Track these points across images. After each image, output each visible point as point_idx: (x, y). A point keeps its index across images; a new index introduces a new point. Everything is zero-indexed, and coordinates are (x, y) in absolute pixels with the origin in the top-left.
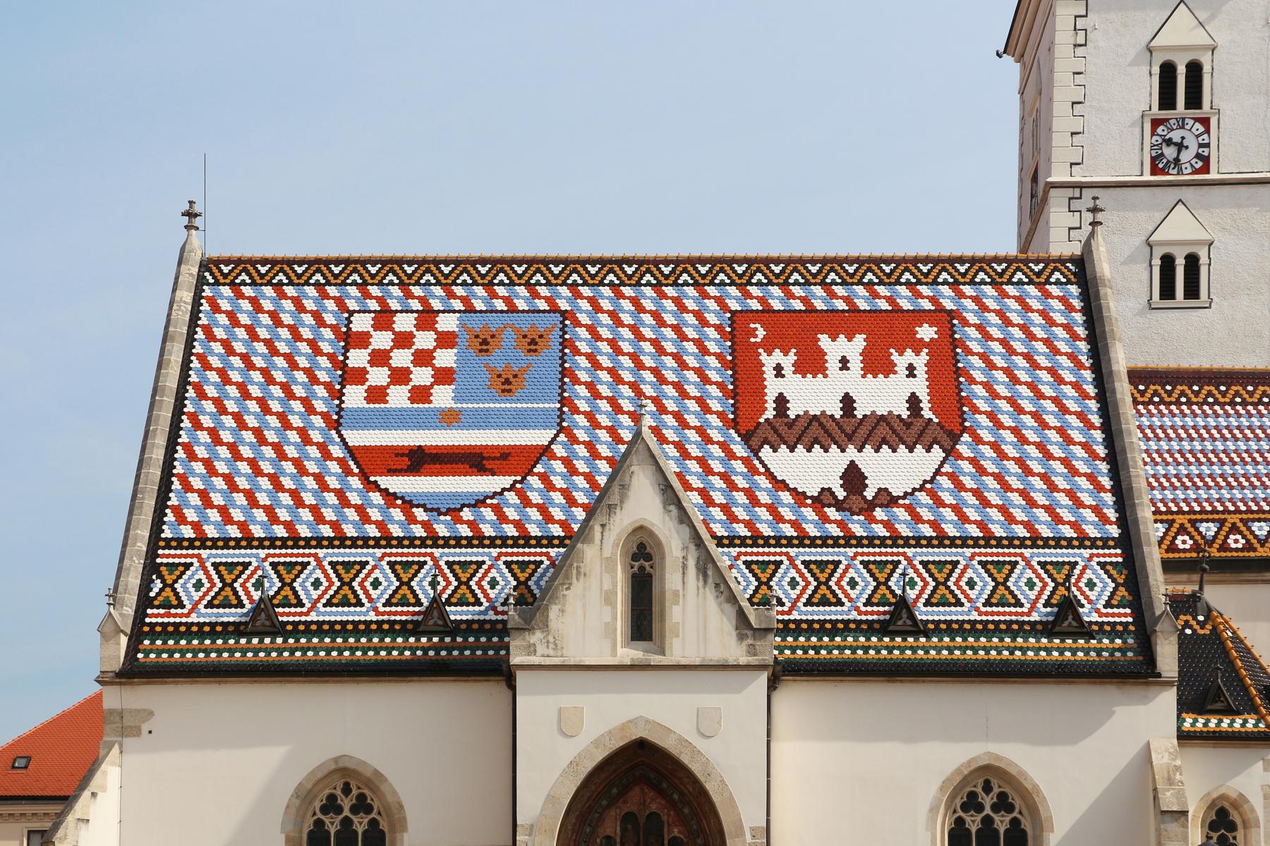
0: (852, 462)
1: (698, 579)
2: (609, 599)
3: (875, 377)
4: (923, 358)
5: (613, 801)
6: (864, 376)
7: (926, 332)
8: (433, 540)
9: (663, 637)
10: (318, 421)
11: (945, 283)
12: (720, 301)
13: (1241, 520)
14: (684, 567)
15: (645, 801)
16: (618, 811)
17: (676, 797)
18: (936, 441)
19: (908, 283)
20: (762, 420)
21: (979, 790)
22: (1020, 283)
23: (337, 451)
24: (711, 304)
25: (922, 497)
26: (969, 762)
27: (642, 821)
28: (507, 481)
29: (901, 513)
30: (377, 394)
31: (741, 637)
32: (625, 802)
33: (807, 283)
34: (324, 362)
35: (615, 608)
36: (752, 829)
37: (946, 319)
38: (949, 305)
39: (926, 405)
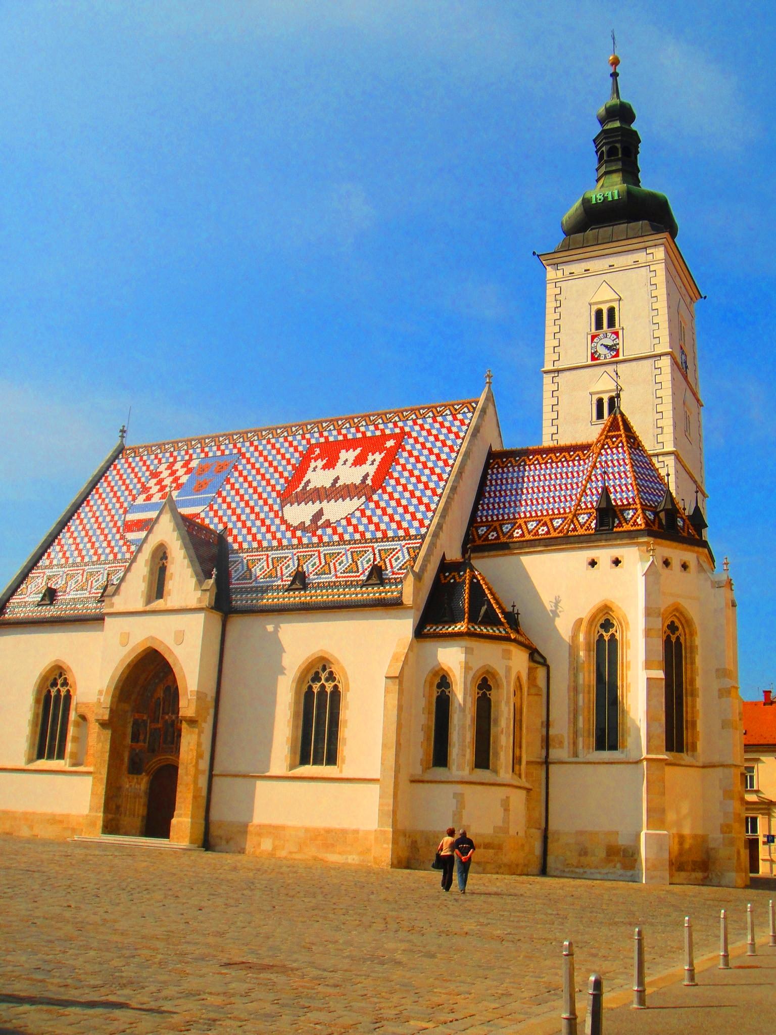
0: (322, 508)
2: (144, 581)
4: (383, 455)
7: (390, 443)
10: (121, 511)
11: (412, 419)
12: (308, 441)
13: (525, 522)
18: (365, 494)
21: (320, 671)
22: (447, 415)
23: (119, 524)
24: (304, 442)
25: (344, 522)
26: (313, 654)
29: (329, 531)
30: (149, 498)
33: (351, 427)
34: (139, 486)
36: (191, 691)
37: (401, 437)
38: (407, 429)
39: (369, 478)
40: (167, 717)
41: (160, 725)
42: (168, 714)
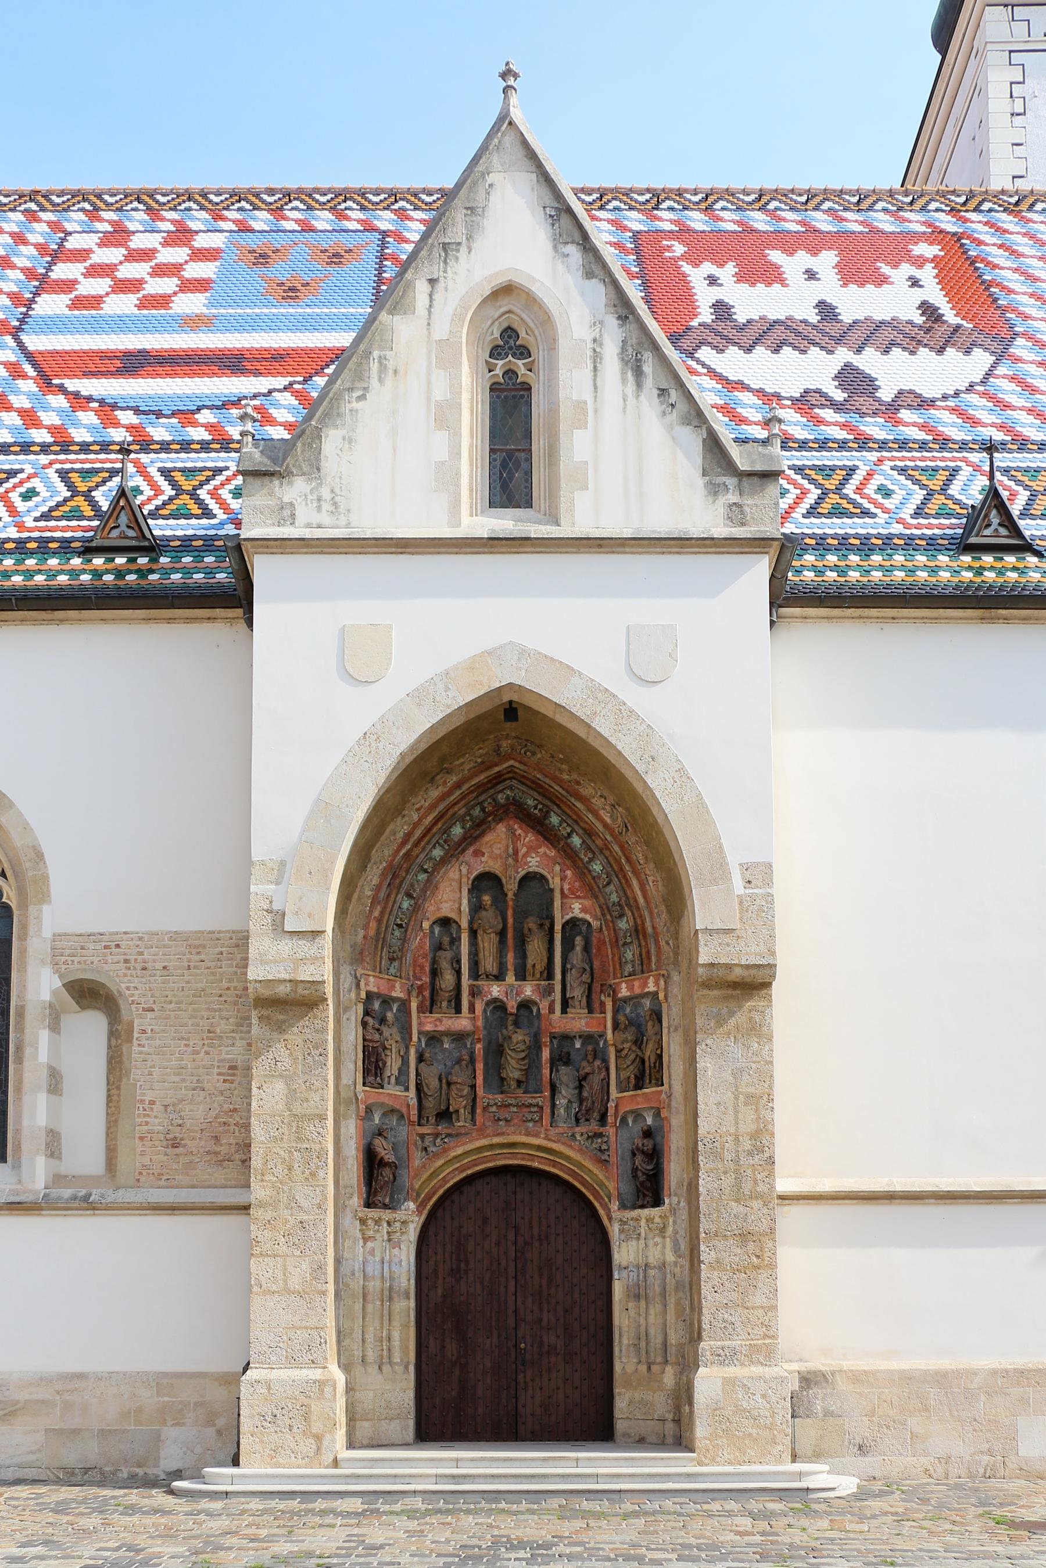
1: (624, 381)
3: (862, 285)
5: (455, 851)
6: (845, 285)
8: (146, 445)
9: (553, 494)
14: (597, 357)
15: (516, 852)
16: (464, 871)
17: (576, 841)
19: (885, 210)
20: (694, 323)
27: (511, 887)
28: (281, 382)
31: (714, 490)
32: (478, 853)
35: (456, 434)
40: (496, 990)
41: (462, 1023)
42: (499, 977)
